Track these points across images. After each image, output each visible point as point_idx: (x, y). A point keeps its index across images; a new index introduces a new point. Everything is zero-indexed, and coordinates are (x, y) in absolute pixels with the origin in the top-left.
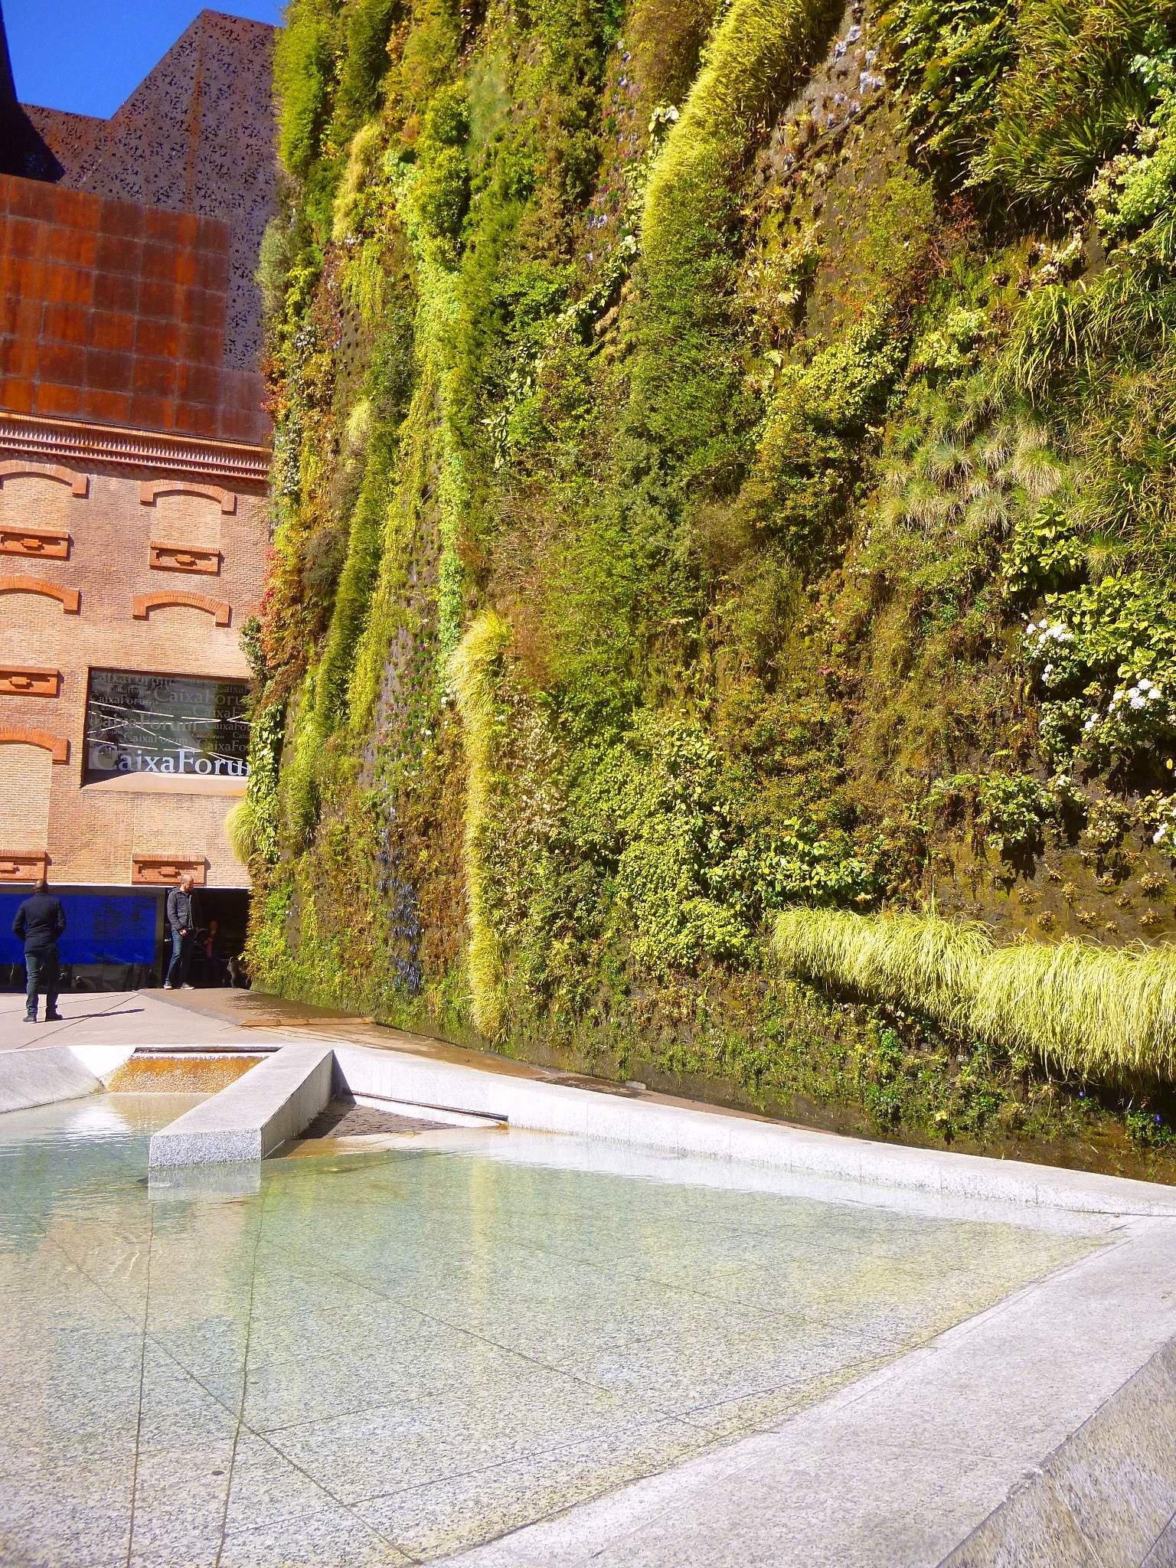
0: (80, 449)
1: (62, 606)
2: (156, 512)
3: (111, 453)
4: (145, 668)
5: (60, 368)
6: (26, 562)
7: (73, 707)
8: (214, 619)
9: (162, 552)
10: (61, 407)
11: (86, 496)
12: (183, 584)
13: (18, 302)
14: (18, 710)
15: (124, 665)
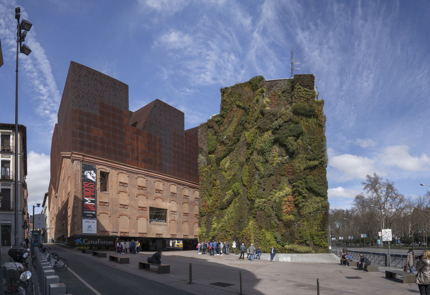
0: (147, 173)
1: (146, 197)
2: (155, 184)
3: (150, 174)
4: (155, 207)
5: (144, 161)
6: (141, 191)
7: (148, 213)
8: (162, 200)
9: (157, 190)
10: (145, 167)
11: (147, 181)
12: (159, 195)
13: (138, 149)
14: (142, 213)
15: (153, 207)
